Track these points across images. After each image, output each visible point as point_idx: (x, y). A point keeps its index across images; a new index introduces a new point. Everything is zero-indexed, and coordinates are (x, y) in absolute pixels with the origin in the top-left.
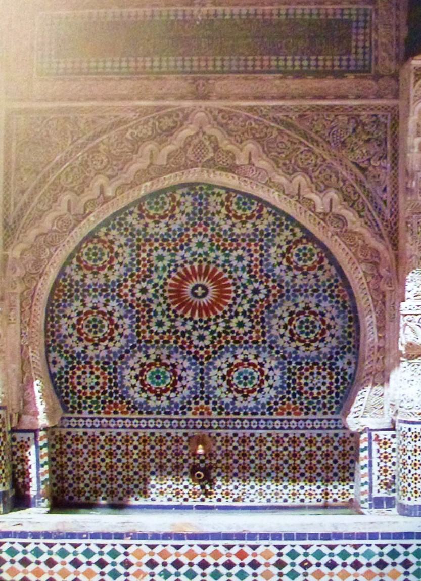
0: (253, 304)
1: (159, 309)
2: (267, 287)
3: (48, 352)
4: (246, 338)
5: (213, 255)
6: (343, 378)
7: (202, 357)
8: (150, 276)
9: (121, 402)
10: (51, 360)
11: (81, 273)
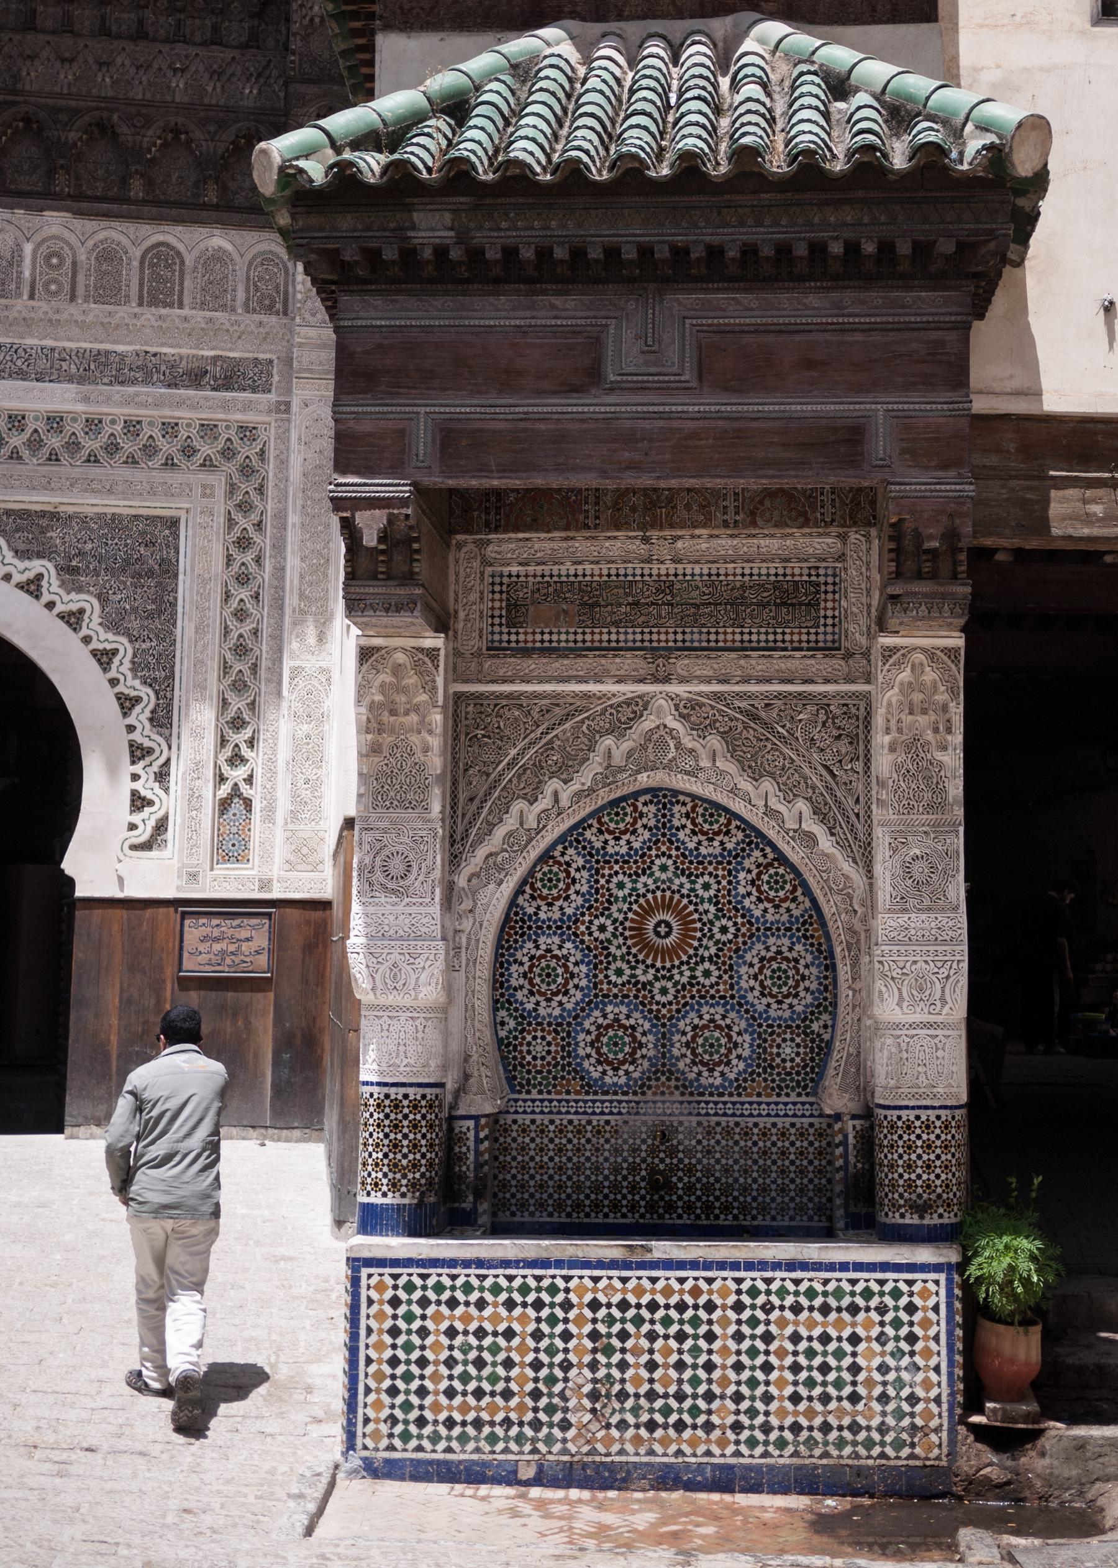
0: (720, 945)
1: (619, 953)
2: (735, 924)
3: (495, 1010)
4: (712, 992)
5: (677, 881)
6: (819, 1047)
7: (664, 1016)
8: (608, 909)
9: (574, 1079)
10: (499, 1020)
11: (534, 904)
